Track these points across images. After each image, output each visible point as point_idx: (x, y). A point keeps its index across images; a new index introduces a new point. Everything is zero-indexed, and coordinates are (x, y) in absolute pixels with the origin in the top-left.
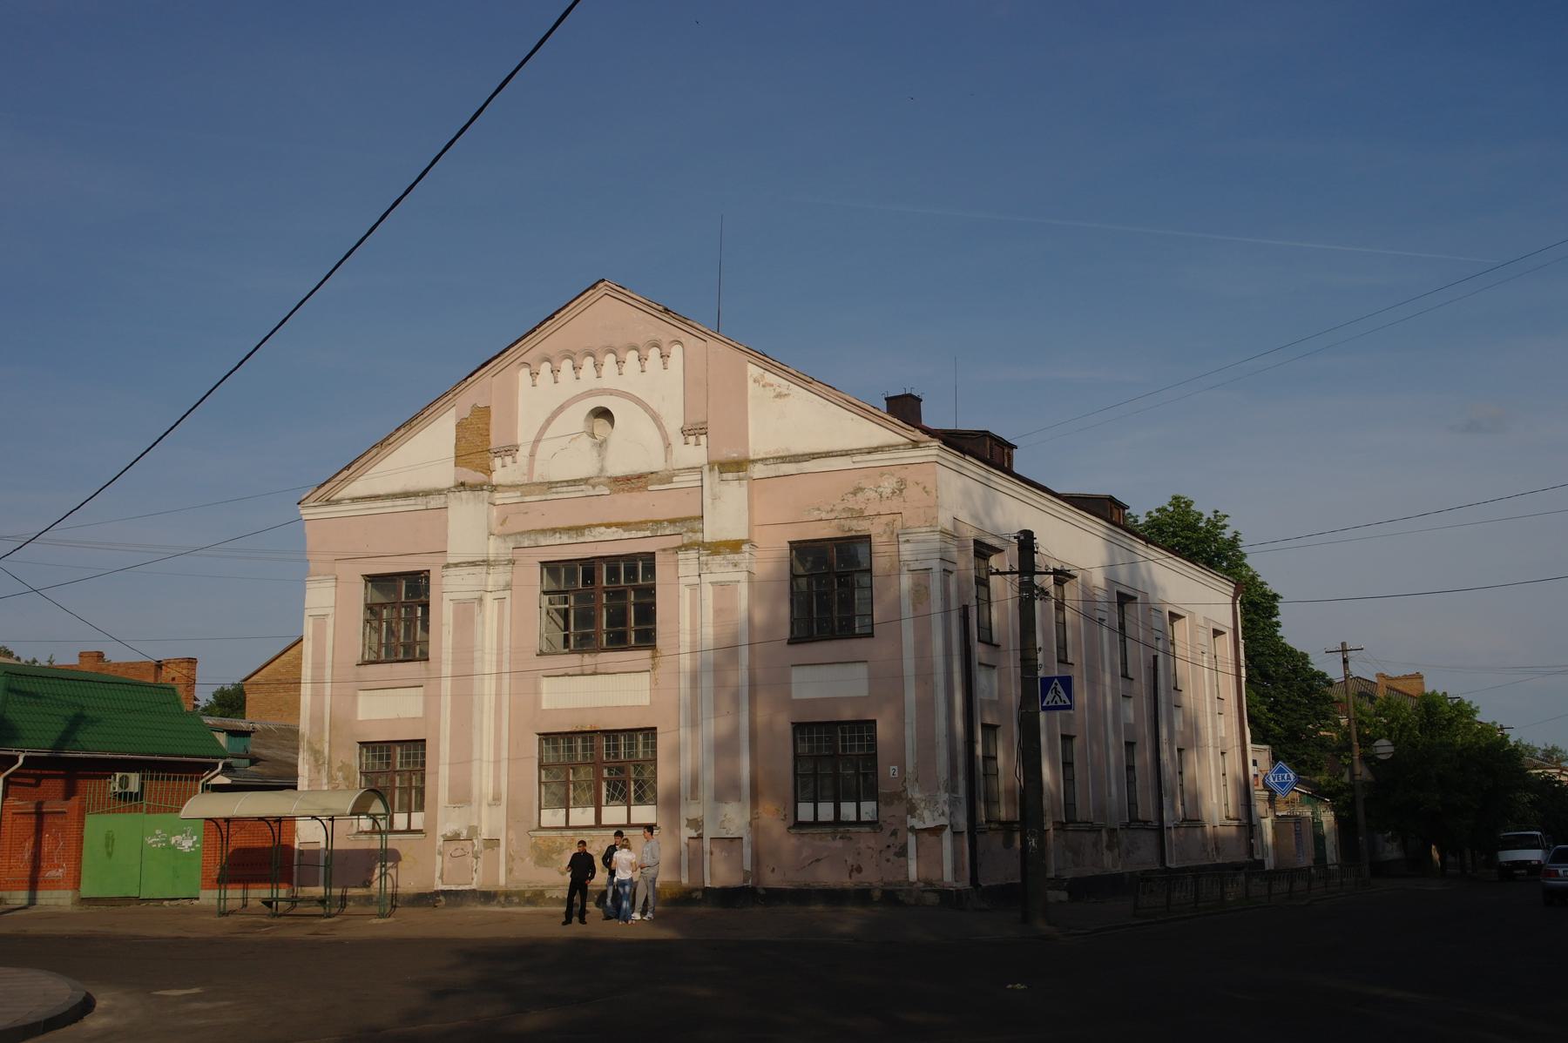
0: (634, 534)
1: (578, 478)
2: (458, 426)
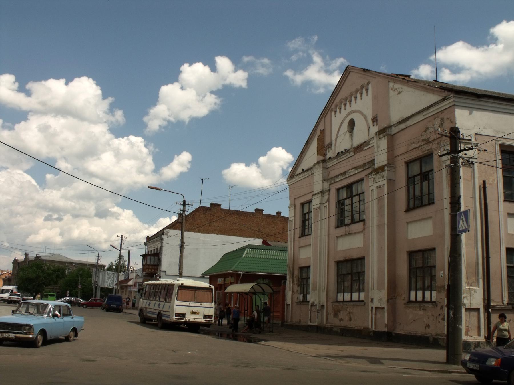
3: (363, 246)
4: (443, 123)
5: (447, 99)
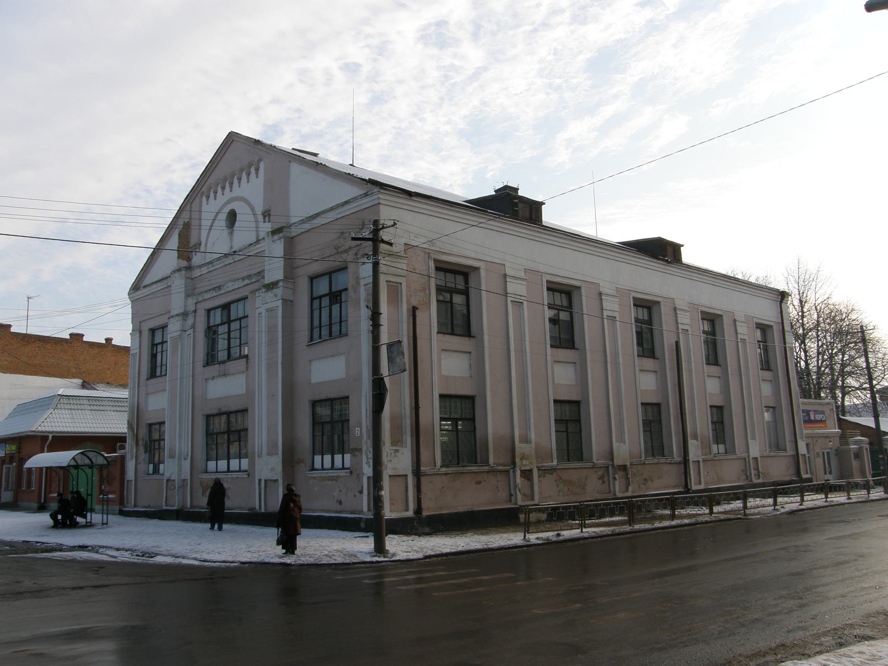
3: (246, 391)
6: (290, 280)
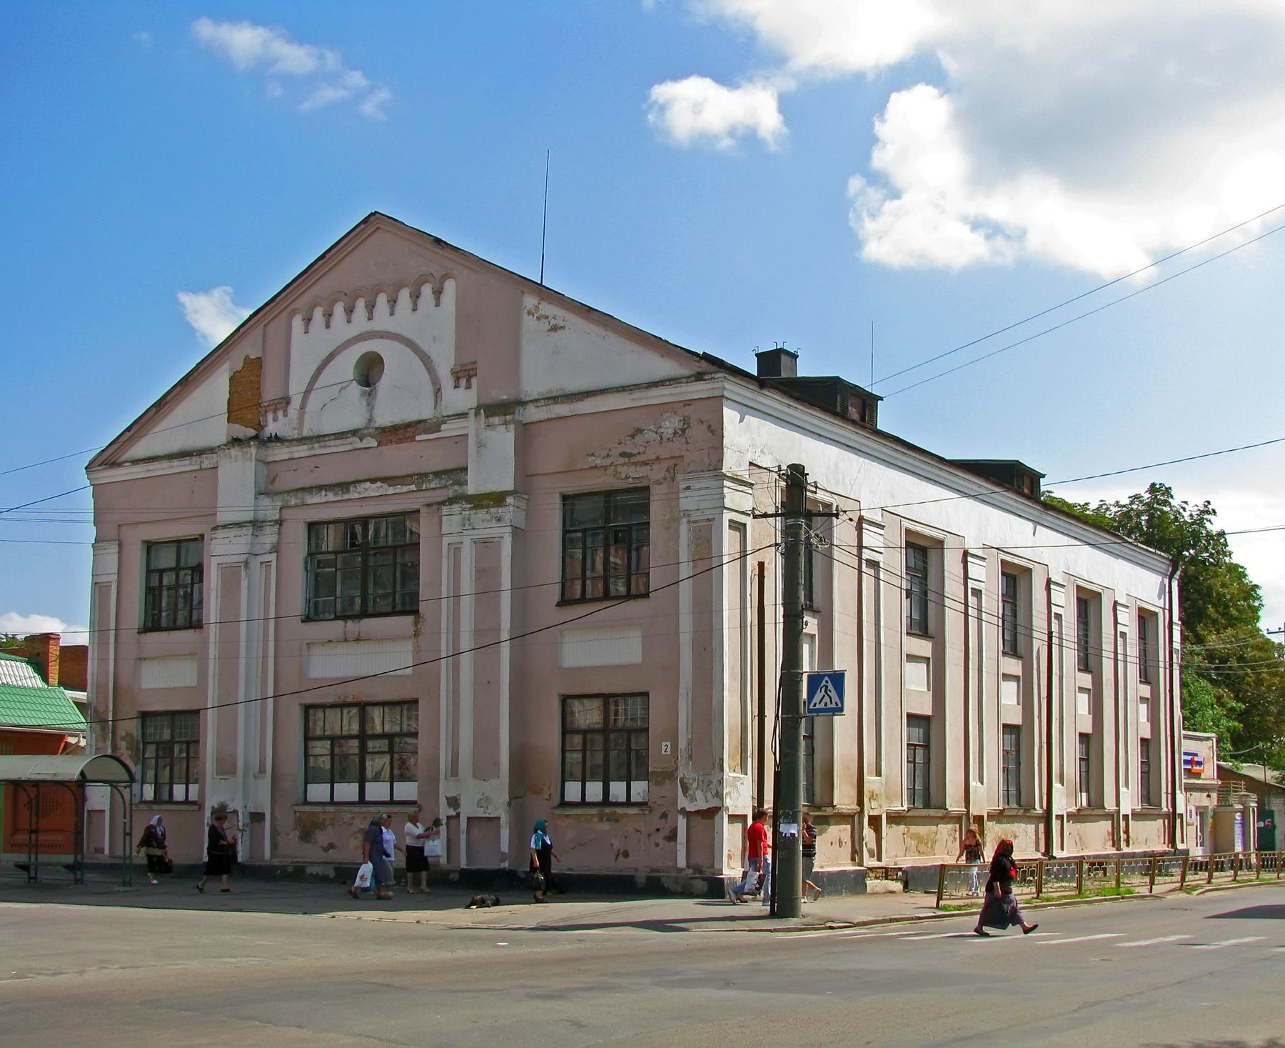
0: (399, 489)
1: (347, 430)
2: (232, 379)
4: (686, 429)
5: (705, 380)
6: (524, 496)
